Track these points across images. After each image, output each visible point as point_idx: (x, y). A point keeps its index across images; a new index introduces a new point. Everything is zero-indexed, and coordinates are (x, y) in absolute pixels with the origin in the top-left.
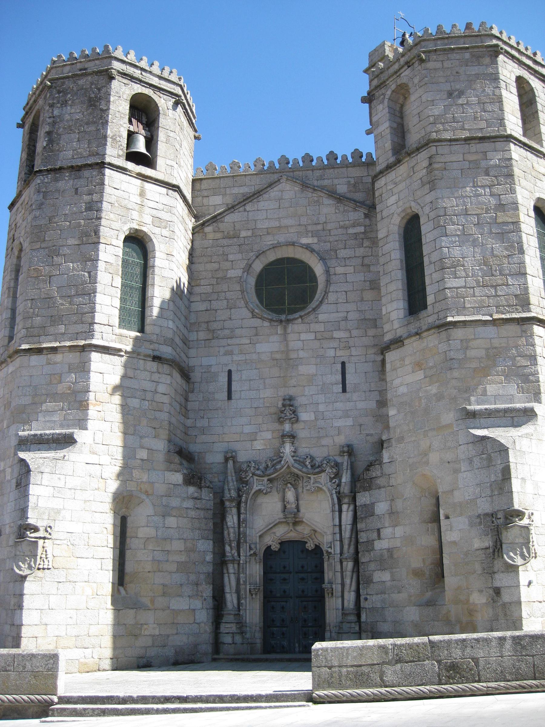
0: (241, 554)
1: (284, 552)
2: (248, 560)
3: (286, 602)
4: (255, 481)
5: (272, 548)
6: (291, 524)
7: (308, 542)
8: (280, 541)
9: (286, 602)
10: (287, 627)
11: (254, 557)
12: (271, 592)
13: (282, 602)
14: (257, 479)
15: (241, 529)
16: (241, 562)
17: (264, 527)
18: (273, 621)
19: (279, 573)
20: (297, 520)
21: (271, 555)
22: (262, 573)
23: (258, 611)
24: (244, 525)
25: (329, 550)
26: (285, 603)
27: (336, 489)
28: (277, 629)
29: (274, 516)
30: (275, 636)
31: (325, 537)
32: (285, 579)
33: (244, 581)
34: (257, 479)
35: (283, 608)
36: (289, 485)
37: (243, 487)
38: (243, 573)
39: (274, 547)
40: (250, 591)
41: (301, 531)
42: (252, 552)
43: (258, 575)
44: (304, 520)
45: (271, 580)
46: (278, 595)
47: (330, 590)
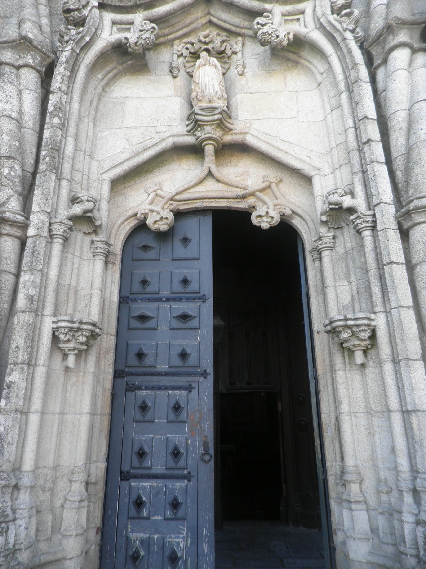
0: (35, 208)
1: (185, 240)
2: (58, 230)
3: (189, 388)
4: (107, 23)
5: (149, 222)
6: (209, 149)
7: (259, 204)
8: (175, 205)
9: (189, 388)
10: (188, 477)
11: (88, 239)
12: (140, 355)
13: (173, 388)
14: (114, 23)
15: (47, 134)
16: (31, 232)
17: (126, 156)
18: (141, 454)
19: (168, 300)
20: (228, 138)
21: (146, 248)
22: (115, 298)
23: (85, 420)
24: (56, 120)
25: (347, 202)
26: (184, 393)
27: (353, 31)
28: (154, 483)
29: (158, 130)
30: (145, 513)
31: (316, 181)
32: (185, 317)
33: (30, 299)
34: (114, 23)
35: (177, 408)
36: (204, 54)
37: (69, 30)
38: (32, 270)
39: (158, 218)
40: (55, 339)
41: (238, 179)
42: (78, 209)
43: (96, 294)
44: (250, 140)
45: (143, 318)
46: (163, 367)
47: (366, 335)
